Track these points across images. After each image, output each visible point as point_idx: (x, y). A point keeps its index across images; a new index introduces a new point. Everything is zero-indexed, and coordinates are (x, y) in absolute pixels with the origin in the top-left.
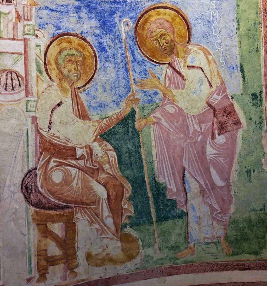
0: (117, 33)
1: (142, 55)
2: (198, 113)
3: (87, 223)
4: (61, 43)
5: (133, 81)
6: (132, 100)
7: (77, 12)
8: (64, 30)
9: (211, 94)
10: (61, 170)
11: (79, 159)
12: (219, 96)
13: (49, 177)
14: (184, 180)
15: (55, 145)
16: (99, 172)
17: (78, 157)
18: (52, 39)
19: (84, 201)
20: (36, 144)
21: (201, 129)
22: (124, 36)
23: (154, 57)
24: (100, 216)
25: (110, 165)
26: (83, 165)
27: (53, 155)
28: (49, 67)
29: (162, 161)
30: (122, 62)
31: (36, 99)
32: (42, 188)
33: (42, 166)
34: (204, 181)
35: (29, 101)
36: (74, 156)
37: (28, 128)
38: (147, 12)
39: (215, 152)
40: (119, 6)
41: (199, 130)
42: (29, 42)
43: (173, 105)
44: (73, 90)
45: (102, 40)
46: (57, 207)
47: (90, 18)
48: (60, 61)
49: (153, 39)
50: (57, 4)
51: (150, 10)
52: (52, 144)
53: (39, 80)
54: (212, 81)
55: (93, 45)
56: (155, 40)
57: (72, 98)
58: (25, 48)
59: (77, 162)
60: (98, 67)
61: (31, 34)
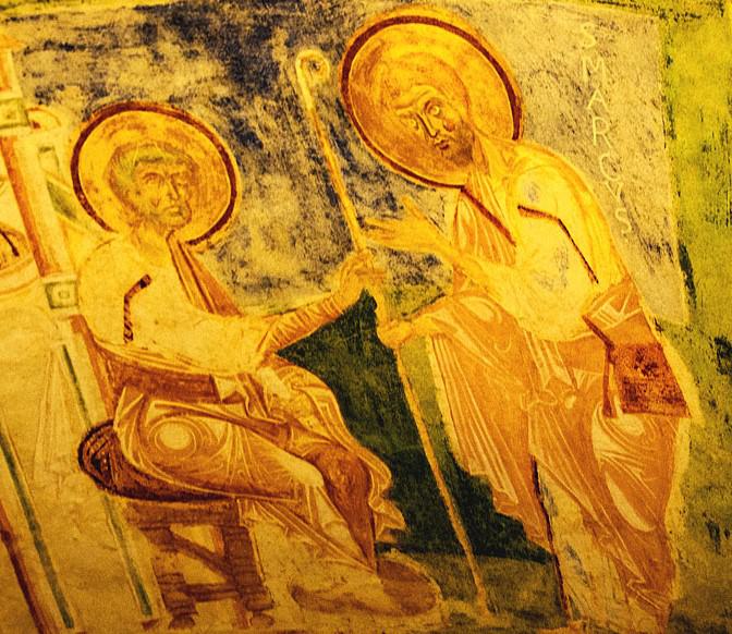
0: (286, 93)
1: (373, 154)
2: (562, 339)
3: (277, 530)
4: (115, 131)
5: (356, 224)
6: (358, 273)
7: (146, 43)
8: (118, 97)
9: (598, 300)
10: (183, 423)
11: (226, 401)
12: (619, 310)
13: (152, 439)
14: (537, 484)
15: (153, 373)
16: (289, 433)
17: (222, 397)
18: (85, 126)
19: (262, 487)
20: (97, 373)
21: (574, 380)
22: (308, 102)
23: (414, 163)
24: (311, 521)
25: (320, 419)
26: (243, 414)
27: (151, 392)
28: (91, 198)
29: (469, 428)
30: (314, 172)
31: (73, 277)
32: (137, 459)
33: (128, 417)
34: (593, 502)
35: (52, 284)
36: (211, 393)
37: (64, 343)
38: (373, 30)
39: (615, 447)
40: (279, 12)
41: (570, 382)
42: (16, 146)
43: (484, 300)
44: (175, 247)
45: (242, 114)
46: (186, 496)
47: (192, 55)
48: (123, 178)
49: (405, 111)
50: (76, 29)
51: (385, 24)
52: (143, 370)
53: (70, 232)
54: (595, 267)
55: (213, 130)
56: (411, 116)
57: (176, 266)
58: (8, 163)
59: (224, 409)
60: (240, 188)
61: (16, 125)
